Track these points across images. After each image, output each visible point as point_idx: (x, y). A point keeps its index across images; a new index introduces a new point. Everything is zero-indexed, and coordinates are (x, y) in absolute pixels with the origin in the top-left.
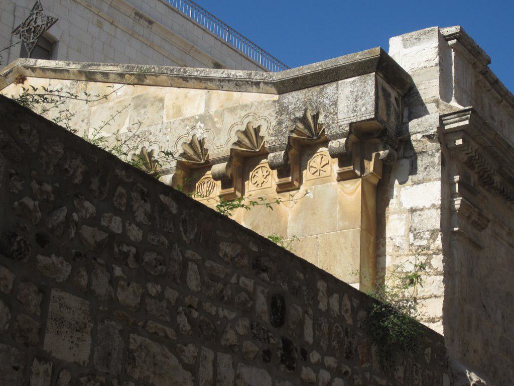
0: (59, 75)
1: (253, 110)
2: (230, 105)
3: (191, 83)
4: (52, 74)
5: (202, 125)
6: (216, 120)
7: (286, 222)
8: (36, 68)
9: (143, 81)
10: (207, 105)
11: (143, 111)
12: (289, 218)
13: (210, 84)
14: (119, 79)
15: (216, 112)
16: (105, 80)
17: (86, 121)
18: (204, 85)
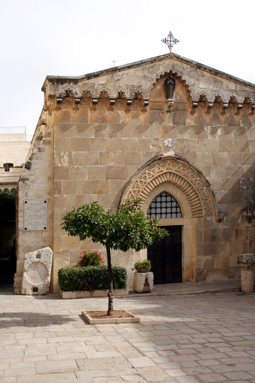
1: (248, 92)
2: (242, 89)
3: (232, 80)
4: (184, 62)
5: (235, 93)
6: (239, 92)
7: (251, 122)
8: (179, 58)
9: (217, 74)
10: (236, 87)
11: (217, 83)
12: (252, 122)
13: (238, 82)
15: (238, 90)
18: (235, 82)
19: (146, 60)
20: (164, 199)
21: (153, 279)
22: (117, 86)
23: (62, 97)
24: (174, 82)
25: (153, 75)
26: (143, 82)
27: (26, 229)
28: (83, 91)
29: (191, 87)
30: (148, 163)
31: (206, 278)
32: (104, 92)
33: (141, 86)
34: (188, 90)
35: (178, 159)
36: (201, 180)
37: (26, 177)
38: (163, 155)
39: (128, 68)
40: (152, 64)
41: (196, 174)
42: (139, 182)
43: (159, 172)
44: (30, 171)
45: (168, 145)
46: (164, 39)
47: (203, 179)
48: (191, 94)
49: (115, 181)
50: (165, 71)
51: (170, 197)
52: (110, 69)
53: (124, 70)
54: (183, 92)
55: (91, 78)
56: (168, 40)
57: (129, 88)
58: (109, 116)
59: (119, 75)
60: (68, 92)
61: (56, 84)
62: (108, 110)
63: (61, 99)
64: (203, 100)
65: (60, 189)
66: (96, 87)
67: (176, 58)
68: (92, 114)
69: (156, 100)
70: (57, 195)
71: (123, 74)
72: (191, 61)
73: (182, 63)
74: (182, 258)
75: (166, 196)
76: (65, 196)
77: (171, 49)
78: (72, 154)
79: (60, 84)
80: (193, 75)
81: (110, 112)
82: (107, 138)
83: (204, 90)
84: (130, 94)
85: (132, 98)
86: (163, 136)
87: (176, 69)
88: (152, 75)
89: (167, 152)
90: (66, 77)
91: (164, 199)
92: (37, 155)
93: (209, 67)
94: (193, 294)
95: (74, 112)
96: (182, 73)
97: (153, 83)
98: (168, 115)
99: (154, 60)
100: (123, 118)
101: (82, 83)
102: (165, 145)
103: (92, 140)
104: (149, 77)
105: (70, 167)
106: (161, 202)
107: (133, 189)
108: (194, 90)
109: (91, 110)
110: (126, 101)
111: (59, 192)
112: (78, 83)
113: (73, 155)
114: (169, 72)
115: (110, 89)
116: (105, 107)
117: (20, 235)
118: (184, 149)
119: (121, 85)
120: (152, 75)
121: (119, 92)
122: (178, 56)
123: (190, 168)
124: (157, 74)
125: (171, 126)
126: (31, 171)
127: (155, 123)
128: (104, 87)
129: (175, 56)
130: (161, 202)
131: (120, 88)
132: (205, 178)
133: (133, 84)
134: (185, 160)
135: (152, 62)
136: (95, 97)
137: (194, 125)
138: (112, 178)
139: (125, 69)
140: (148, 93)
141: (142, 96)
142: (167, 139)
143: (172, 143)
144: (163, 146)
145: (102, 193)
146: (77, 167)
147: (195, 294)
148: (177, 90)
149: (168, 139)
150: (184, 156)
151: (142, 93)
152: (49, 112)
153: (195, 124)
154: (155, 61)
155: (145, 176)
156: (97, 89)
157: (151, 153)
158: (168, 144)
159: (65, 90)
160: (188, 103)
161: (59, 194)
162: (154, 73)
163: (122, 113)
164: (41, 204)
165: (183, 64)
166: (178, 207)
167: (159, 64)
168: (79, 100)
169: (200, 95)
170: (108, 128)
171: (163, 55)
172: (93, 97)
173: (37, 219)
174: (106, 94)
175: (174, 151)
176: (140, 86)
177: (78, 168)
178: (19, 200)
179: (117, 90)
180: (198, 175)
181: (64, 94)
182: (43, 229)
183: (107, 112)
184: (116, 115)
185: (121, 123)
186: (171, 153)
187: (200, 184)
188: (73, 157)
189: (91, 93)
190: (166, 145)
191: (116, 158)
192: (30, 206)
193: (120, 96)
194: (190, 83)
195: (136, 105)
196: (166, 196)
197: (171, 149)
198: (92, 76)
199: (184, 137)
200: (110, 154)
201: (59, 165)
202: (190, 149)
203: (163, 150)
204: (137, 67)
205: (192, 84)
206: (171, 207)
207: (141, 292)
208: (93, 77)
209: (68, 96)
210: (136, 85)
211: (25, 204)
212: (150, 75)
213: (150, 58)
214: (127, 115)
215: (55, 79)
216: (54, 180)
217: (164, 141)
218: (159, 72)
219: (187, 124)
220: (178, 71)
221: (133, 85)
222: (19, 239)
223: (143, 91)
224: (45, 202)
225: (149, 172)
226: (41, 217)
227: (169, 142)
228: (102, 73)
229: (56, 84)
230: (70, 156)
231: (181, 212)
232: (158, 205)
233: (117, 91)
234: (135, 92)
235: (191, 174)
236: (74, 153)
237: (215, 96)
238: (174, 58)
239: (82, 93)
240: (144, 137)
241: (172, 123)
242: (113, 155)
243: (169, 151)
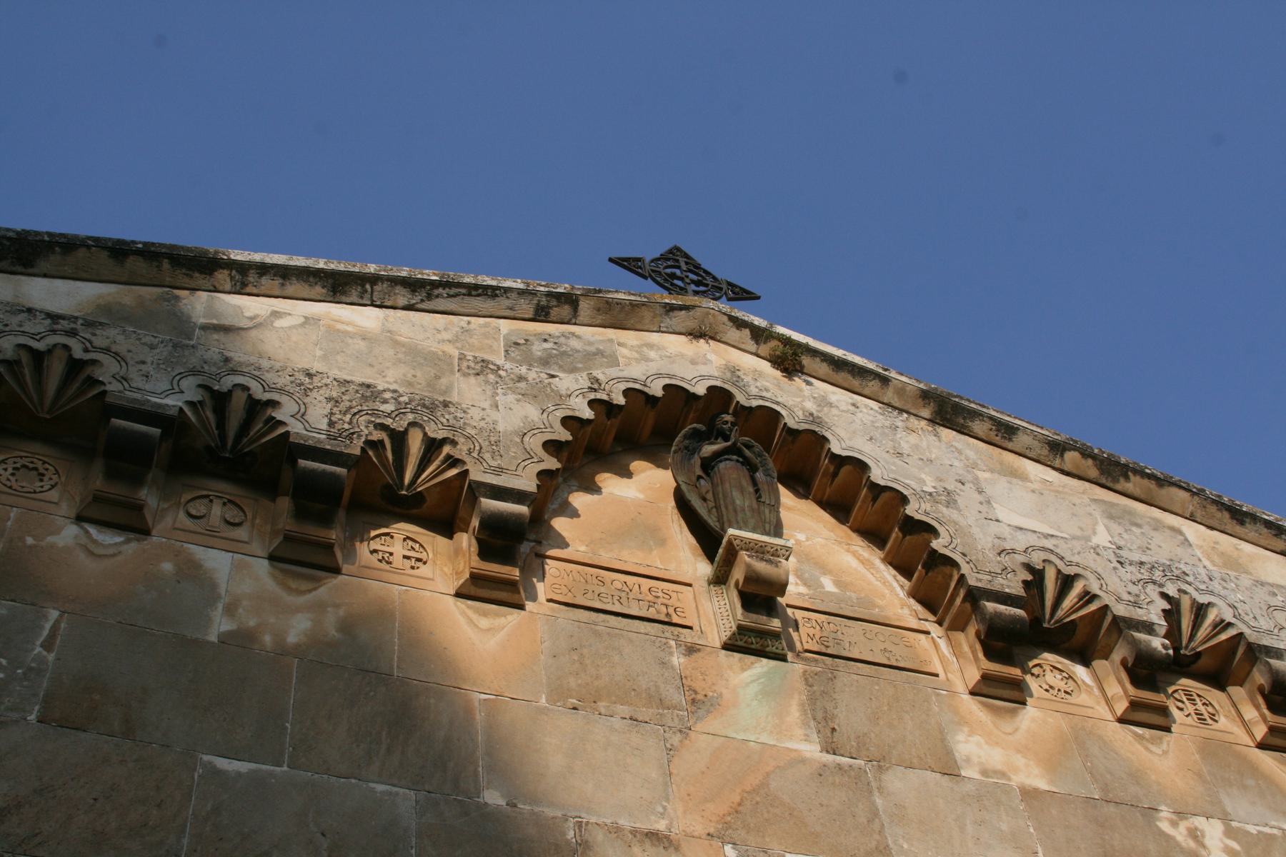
0: (842, 377)
3: (1249, 530)
9: (1116, 481)
14: (1045, 451)
16: (998, 440)
32: (56, 369)
39: (319, 290)
50: (668, 381)
52: (145, 244)
53: (291, 289)
58: (82, 556)
62: (80, 519)
64: (1060, 613)
67: (747, 332)
69: (605, 558)
71: (276, 314)
80: (916, 447)
83: (1048, 544)
86: (728, 825)
87: (764, 394)
88: (553, 376)
100: (245, 603)
104: (521, 378)
115: (128, 356)
120: (553, 376)
125: (803, 761)
127: (624, 710)
128: (72, 333)
131: (234, 372)
135: (541, 314)
137: (1043, 785)
139: (294, 287)
151: (454, 443)
153: (1051, 782)
154: (566, 310)
160: (933, 634)
162: (573, 370)
169: (1029, 567)
179: (194, 372)
184: (167, 567)
185: (213, 638)
194: (907, 481)
218: (613, 372)
219: (977, 769)
220: (778, 403)
233: (189, 383)
234: (388, 421)
237: (1165, 596)
238: (733, 334)
241: (807, 739)
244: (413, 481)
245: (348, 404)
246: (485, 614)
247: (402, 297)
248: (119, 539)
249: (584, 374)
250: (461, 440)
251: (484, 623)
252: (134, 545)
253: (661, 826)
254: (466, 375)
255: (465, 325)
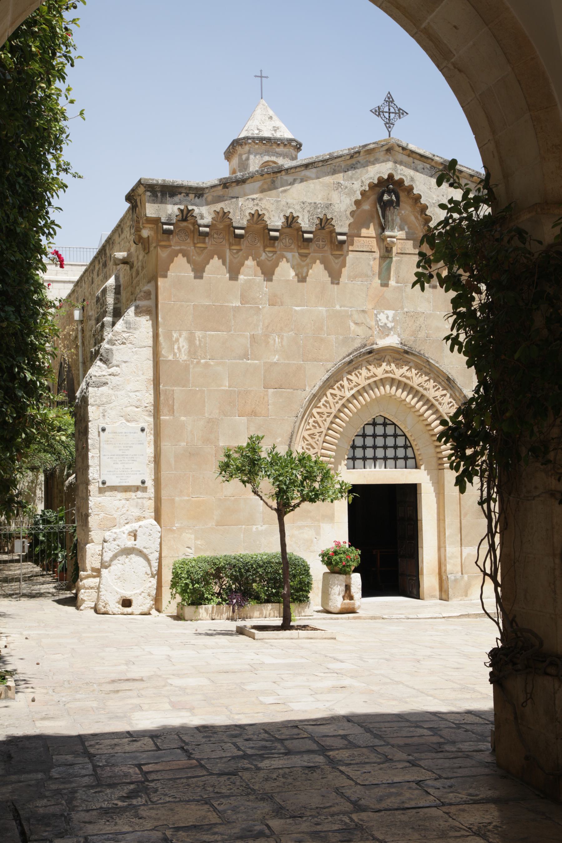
4: (418, 157)
8: (406, 149)
17: (445, 196)
19: (341, 153)
20: (380, 430)
21: (360, 587)
22: (283, 203)
23: (172, 222)
24: (398, 197)
25: (355, 183)
26: (335, 197)
27: (104, 483)
28: (215, 211)
29: (432, 209)
30: (347, 359)
31: (469, 592)
33: (331, 204)
34: (426, 215)
35: (406, 352)
36: (454, 395)
37: (104, 380)
38: (376, 344)
39: (303, 168)
40: (353, 161)
41: (443, 383)
42: (329, 395)
43: (368, 378)
44: (109, 368)
45: (386, 324)
46: (377, 109)
47: (457, 394)
48: (432, 222)
49: (282, 391)
50: (379, 175)
51: (393, 426)
53: (297, 170)
54: (416, 218)
55: (230, 185)
56: (385, 110)
57: (308, 209)
59: (287, 180)
60: (185, 212)
61: (159, 195)
62: (264, 251)
63: (172, 227)
65: (173, 406)
66: (240, 204)
67: (401, 148)
68: (234, 257)
70: (167, 418)
72: (430, 156)
73: (414, 158)
74: (420, 549)
75: (385, 425)
76: (183, 418)
77: (390, 129)
78: (195, 336)
79: (168, 196)
81: (270, 255)
82: (266, 309)
84: (309, 221)
85: (314, 229)
87: (402, 172)
88: (353, 184)
89: (384, 338)
90: (180, 183)
91: (380, 430)
92: (124, 335)
93: (467, 168)
94: (439, 618)
95: (197, 253)
96: (412, 179)
97: (354, 200)
98: (386, 263)
99: (356, 153)
101: (213, 196)
102: (380, 324)
103: (236, 309)
104: (346, 187)
105: (192, 362)
106: (374, 436)
107: (319, 410)
108: (437, 214)
109: (230, 249)
110: (301, 233)
111: (172, 411)
112: (205, 196)
113: (197, 339)
114: (386, 177)
116: (259, 244)
117: (91, 493)
118: (420, 333)
119: (290, 201)
120: (353, 184)
121: (287, 215)
122: (404, 145)
123: (430, 369)
124: (362, 182)
126: (113, 366)
127: (360, 279)
128: (257, 205)
129: (399, 146)
130: (374, 436)
132: (461, 392)
133: (315, 201)
134: (419, 356)
135: (352, 157)
136: (240, 225)
138: (277, 387)
139: (298, 169)
140: (344, 218)
141: (334, 226)
142: (383, 312)
143: (394, 320)
144: (376, 325)
145: (255, 415)
146: (206, 363)
147: (444, 617)
148: (403, 212)
149: (386, 312)
150: (419, 346)
152: (145, 246)
154: (358, 154)
155: (341, 385)
156: (244, 208)
157: (353, 339)
158: (386, 321)
159: (179, 209)
161: (171, 415)
162: (357, 179)
163: (293, 256)
164: (135, 433)
165: (416, 161)
166: (409, 447)
167: (365, 160)
168: (207, 229)
170: (266, 288)
171: (374, 143)
172: (235, 224)
173: (127, 463)
174: (260, 218)
175: (399, 336)
176: (328, 206)
177: (207, 365)
178: (90, 424)
179: (282, 211)
180: (448, 385)
181: (177, 216)
182: (140, 484)
183: (264, 254)
186: (392, 341)
187: (451, 402)
188: (198, 343)
189: (230, 216)
190: (382, 323)
191: (282, 346)
192: (111, 436)
193: (289, 222)
195: (321, 243)
196: (385, 425)
197: (392, 333)
198: (232, 182)
199: (419, 309)
200: (271, 337)
201: (171, 358)
202: (431, 332)
203: (375, 333)
204: (323, 165)
205: (434, 201)
206: (395, 447)
207: (337, 612)
208: (234, 184)
209: (184, 219)
210: (320, 202)
211: (101, 433)
212: (347, 184)
213: (349, 149)
214: (304, 261)
215: (157, 185)
216: (161, 387)
217: (378, 316)
218: (367, 176)
220: (404, 175)
221: (315, 203)
222: (90, 502)
223: (336, 214)
224: (143, 430)
225: (349, 377)
226: (135, 459)
227: (387, 317)
228: (252, 177)
229: (159, 195)
230: (191, 340)
231: (414, 458)
232: (369, 441)
233: (282, 215)
235: (434, 382)
236: (198, 334)
239: (213, 215)
240: (338, 307)
242: (277, 339)
243: (388, 335)
244: (324, 227)
245: (311, 212)
246: (336, 258)
247: (320, 164)
248: (272, 254)
249: (360, 180)
250: (334, 218)
251: (336, 261)
252: (275, 255)
253: (364, 308)
254: (334, 191)
255: (334, 167)
